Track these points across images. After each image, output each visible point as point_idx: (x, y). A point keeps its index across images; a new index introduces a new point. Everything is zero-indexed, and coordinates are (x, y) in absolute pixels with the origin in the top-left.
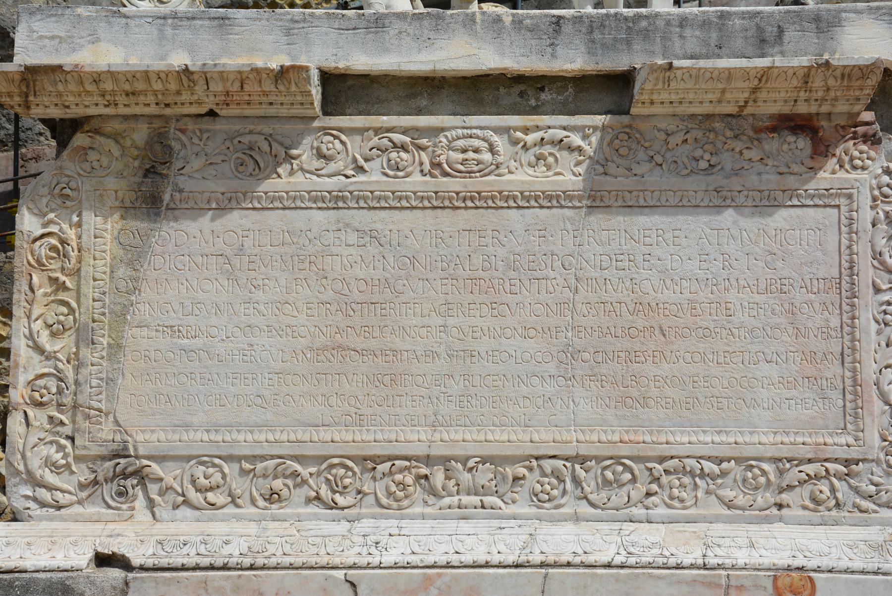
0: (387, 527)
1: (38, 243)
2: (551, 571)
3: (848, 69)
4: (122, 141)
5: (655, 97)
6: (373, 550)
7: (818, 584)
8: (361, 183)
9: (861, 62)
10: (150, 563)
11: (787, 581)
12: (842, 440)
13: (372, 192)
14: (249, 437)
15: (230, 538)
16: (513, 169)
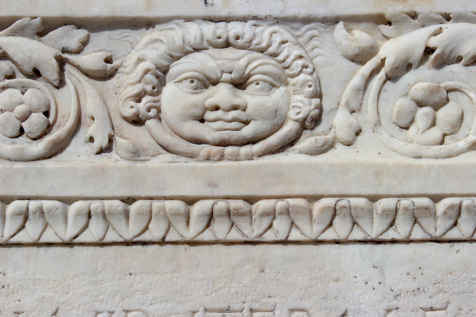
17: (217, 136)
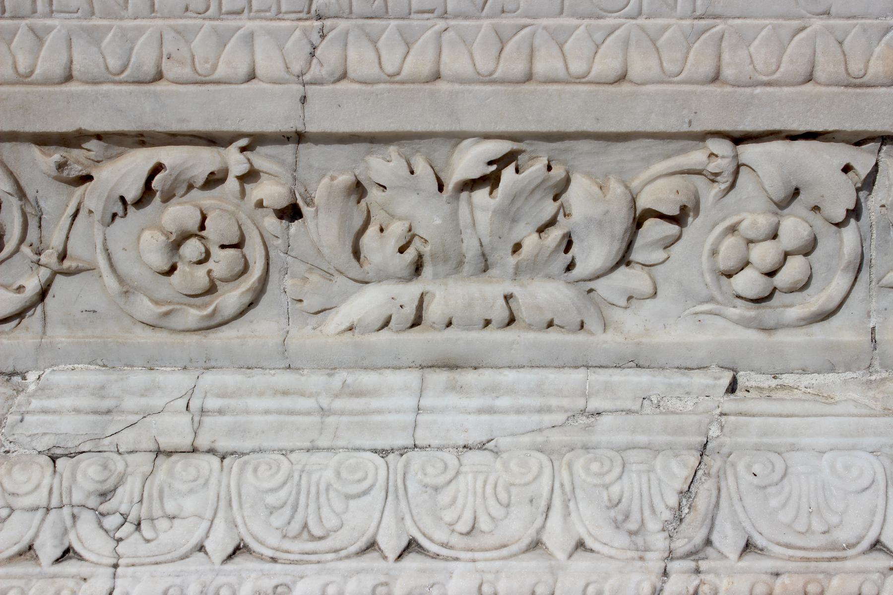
0: (147, 413)
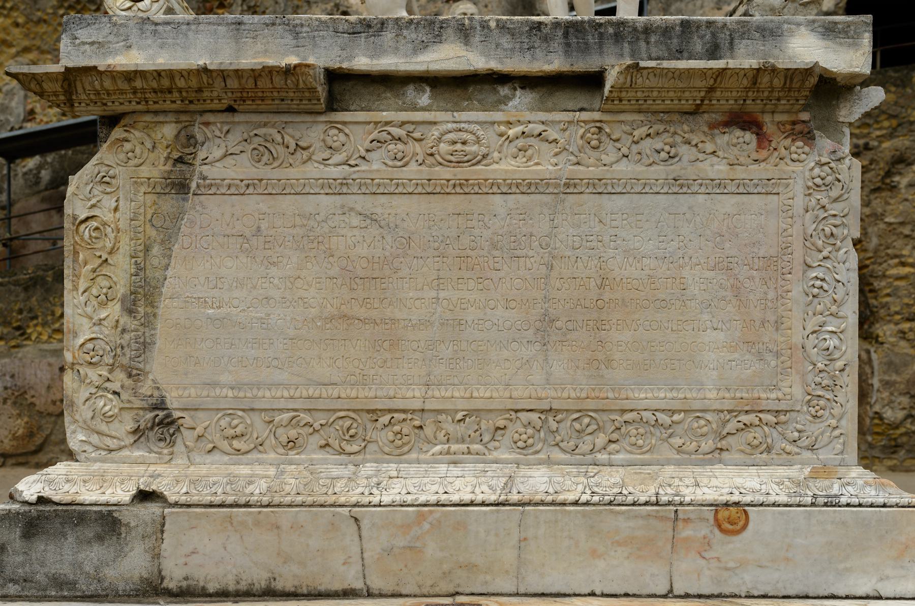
1: (83, 226)
2: (527, 508)
3: (791, 72)
4: (153, 135)
5: (624, 94)
6: (375, 491)
7: (752, 516)
8: (364, 171)
9: (802, 66)
10: (183, 499)
11: (726, 513)
12: (773, 396)
13: (372, 180)
14: (268, 394)
15: (253, 479)
16: (496, 159)
17: (456, 160)
